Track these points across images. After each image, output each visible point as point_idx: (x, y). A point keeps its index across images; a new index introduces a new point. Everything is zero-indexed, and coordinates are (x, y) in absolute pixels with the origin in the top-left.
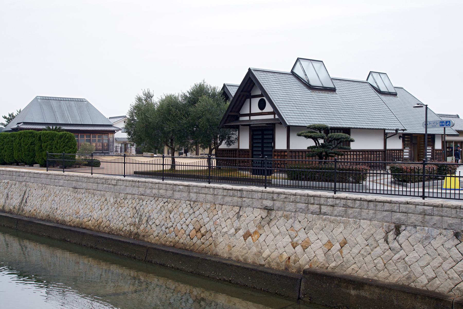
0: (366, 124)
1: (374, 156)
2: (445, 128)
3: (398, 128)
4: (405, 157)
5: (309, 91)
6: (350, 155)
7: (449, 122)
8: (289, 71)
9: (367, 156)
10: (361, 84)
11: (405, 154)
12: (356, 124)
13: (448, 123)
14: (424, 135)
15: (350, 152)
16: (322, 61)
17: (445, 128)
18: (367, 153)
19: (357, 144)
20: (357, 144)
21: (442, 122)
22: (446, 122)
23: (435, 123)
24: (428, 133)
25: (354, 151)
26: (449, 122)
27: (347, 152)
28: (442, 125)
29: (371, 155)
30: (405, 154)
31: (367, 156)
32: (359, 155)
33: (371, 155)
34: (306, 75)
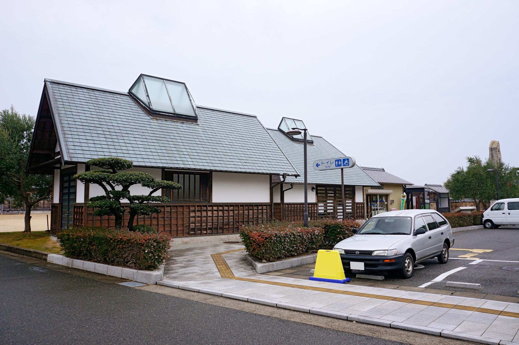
0: (234, 166)
1: (253, 212)
2: (342, 169)
3: (286, 172)
4: (319, 211)
5: (148, 118)
6: (212, 211)
7: (348, 159)
8: (126, 91)
9: (241, 212)
10: (245, 117)
11: (319, 208)
12: (214, 165)
13: (346, 162)
14: (339, 186)
15: (212, 206)
16: (184, 83)
17: (342, 169)
18: (241, 208)
19: (222, 194)
20: (222, 194)
21: (338, 161)
22: (344, 160)
23: (329, 163)
24: (345, 184)
25: (218, 205)
26: (348, 159)
27: (206, 206)
28: (339, 165)
29: (248, 210)
30: (319, 208)
31: (241, 212)
32: (223, 211)
33: (248, 210)
34: (148, 96)
